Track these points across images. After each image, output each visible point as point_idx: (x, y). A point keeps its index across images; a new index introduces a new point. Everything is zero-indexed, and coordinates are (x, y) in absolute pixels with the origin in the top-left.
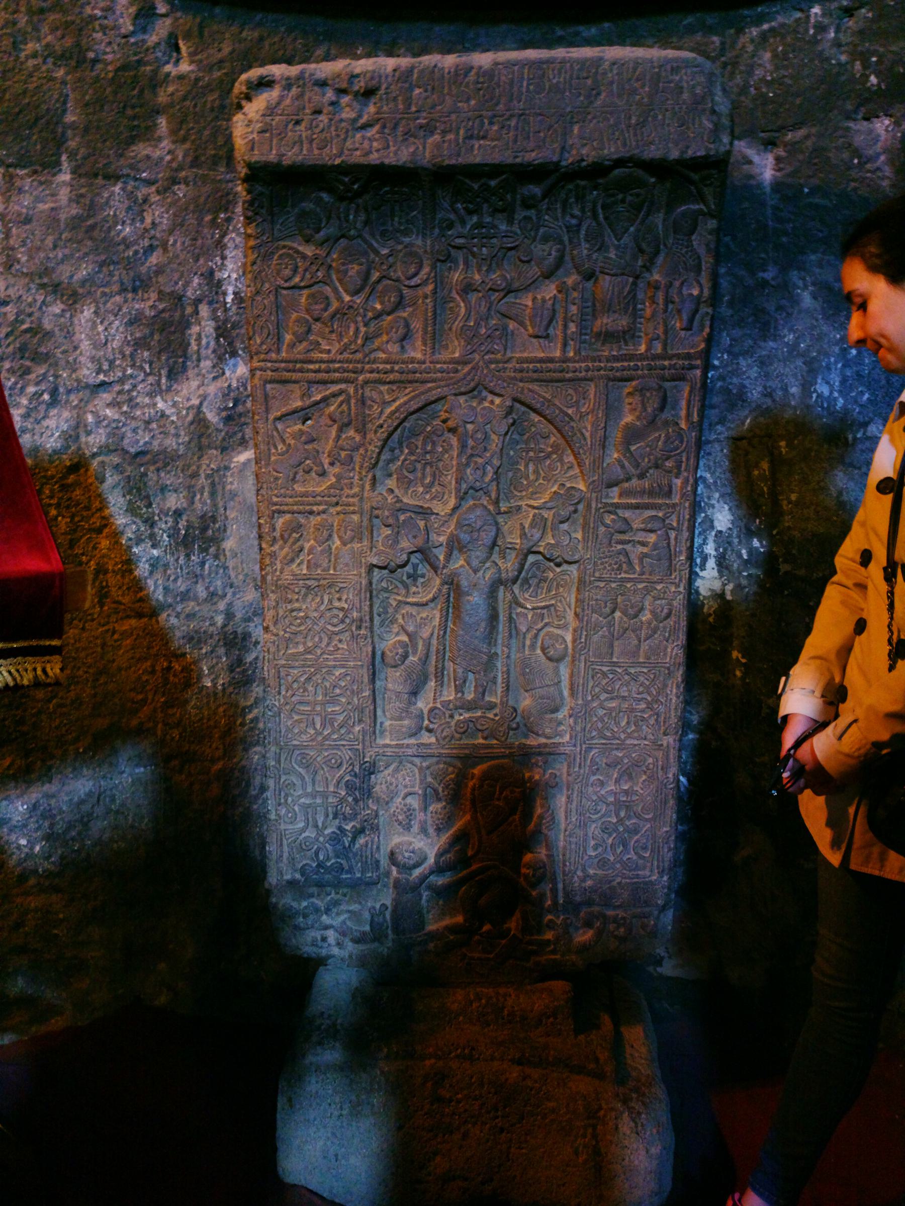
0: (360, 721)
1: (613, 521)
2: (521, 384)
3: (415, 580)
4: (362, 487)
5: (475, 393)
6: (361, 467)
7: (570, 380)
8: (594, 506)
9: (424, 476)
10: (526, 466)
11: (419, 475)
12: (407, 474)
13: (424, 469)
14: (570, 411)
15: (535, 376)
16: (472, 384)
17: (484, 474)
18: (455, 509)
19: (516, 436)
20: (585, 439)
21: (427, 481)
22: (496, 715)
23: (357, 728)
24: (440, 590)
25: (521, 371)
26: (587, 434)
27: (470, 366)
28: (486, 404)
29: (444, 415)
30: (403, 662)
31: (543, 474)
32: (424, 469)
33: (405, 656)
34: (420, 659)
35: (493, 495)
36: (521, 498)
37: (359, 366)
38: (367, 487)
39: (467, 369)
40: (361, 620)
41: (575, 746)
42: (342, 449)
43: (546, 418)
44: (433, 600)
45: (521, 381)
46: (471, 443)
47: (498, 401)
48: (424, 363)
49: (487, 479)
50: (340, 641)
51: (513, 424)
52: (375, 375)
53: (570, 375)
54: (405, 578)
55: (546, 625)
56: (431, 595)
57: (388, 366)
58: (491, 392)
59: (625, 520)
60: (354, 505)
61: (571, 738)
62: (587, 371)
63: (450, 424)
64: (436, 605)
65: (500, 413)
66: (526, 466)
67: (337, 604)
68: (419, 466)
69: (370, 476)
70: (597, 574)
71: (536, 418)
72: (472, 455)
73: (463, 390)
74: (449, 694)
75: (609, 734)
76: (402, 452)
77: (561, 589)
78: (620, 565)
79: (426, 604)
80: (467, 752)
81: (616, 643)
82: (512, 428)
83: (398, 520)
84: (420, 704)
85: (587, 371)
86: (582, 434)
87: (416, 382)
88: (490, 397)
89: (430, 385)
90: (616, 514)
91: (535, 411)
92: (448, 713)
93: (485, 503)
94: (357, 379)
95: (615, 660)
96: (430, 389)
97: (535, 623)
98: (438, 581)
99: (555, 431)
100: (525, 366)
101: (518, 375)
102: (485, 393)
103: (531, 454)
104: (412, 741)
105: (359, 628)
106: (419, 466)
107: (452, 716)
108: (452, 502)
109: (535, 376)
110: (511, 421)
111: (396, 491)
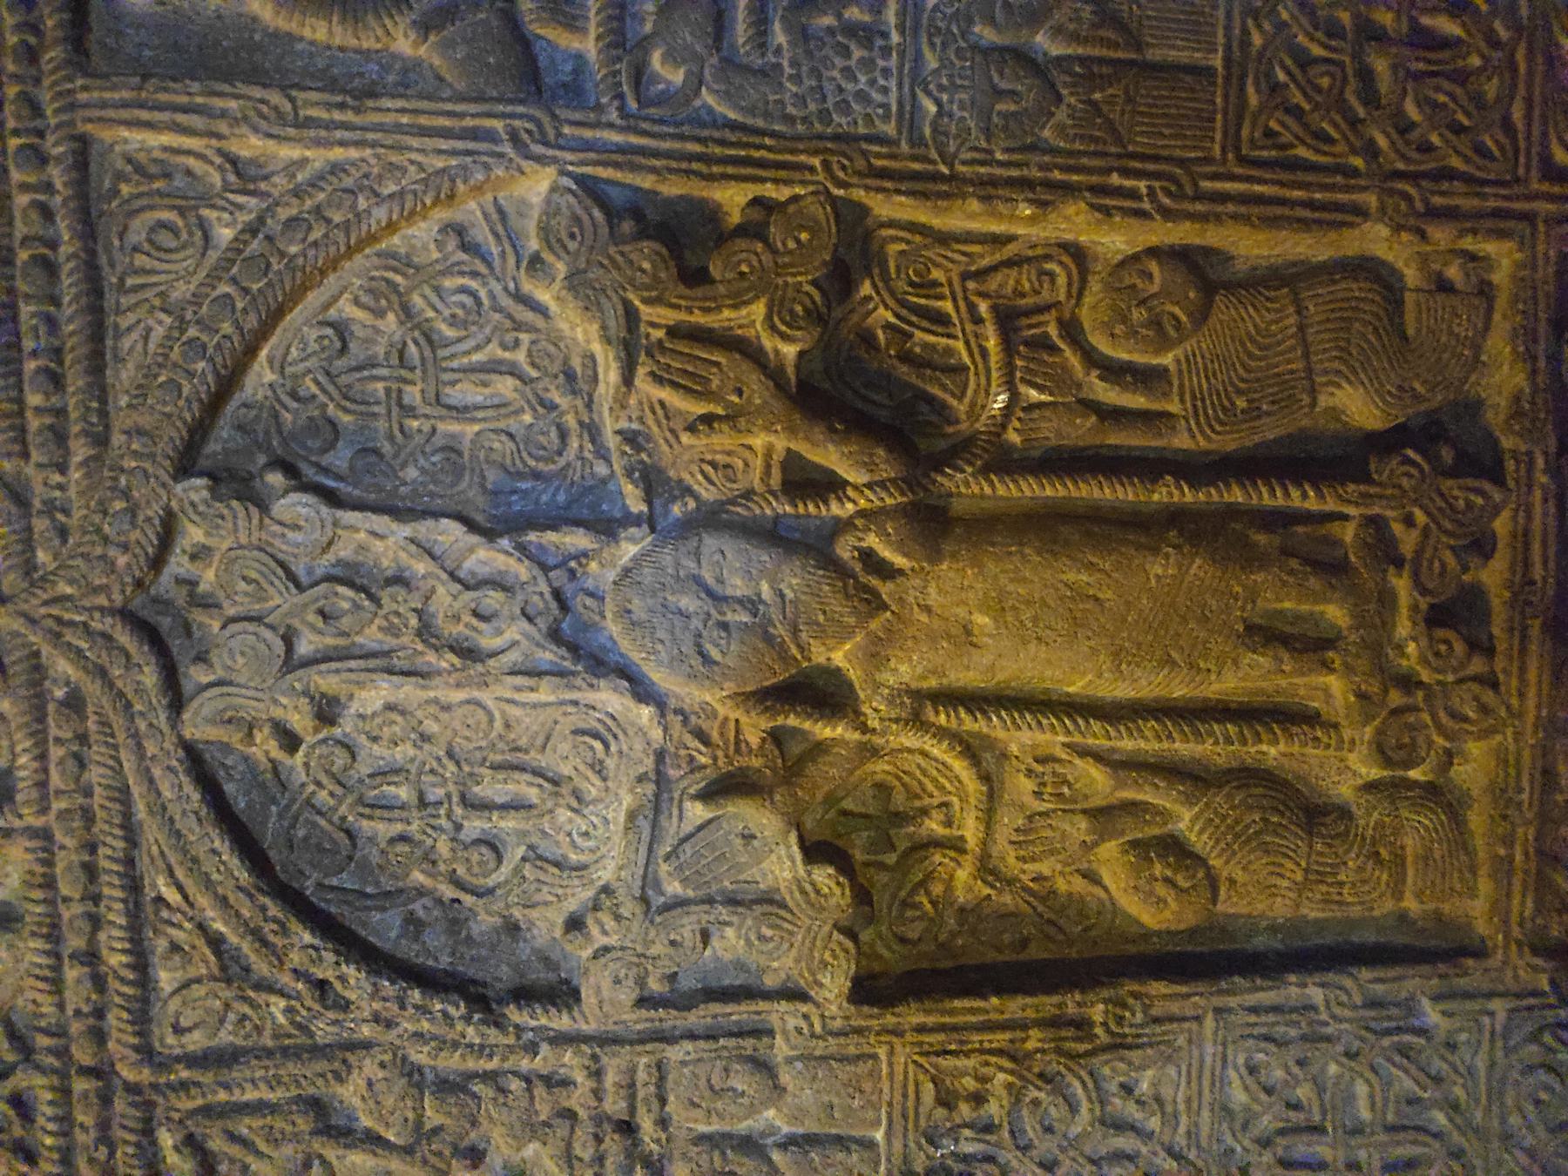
0: (1409, 1006)
1: (671, 57)
2: (117, 439)
3: (899, 818)
4: (562, 1040)
5: (165, 623)
6: (482, 1050)
7: (88, 230)
8: (616, 138)
9: (516, 806)
10: (462, 412)
11: (508, 824)
12: (505, 870)
13: (485, 807)
14: (225, 234)
15: (76, 380)
16: (124, 638)
17: (498, 583)
18: (642, 691)
19: (340, 459)
20: (336, 169)
21: (533, 794)
22: (1409, 521)
23: (1432, 1015)
24: (941, 733)
25: (59, 436)
26: (319, 158)
27: (46, 650)
28: (208, 578)
29: (265, 747)
30: (1200, 861)
31: (494, 350)
32: (485, 807)
33: (1174, 848)
34: (1189, 801)
35: (577, 540)
36: (592, 431)
37: (80, 1085)
38: (562, 1022)
39: (63, 667)
40: (1054, 1023)
41: (1529, 217)
42: (419, 1124)
43: (264, 332)
44: (970, 749)
45: (101, 440)
46: (372, 637)
47: (193, 534)
48: (45, 835)
49: (522, 571)
50: (1127, 1089)
51: (290, 470)
52: (116, 1019)
53: (64, 228)
54: (891, 859)
55: (1072, 330)
56: (959, 766)
57: (72, 973)
58: (157, 563)
60: (632, 1071)
61: (1502, 235)
62: (43, 160)
63: (299, 720)
64: (989, 743)
65: (239, 523)
66: (462, 412)
67: (993, 1109)
68: (475, 826)
69: (515, 1015)
70: (890, 129)
71: (261, 376)
72: (426, 631)
73: (150, 677)
74: (1331, 689)
75: (1491, 89)
76: (421, 892)
77: (936, 274)
78: (851, 30)
79: (986, 778)
80: (1535, 627)
81: (1154, 55)
82: (309, 472)
83: (680, 903)
84: (1345, 791)
85: (43, 160)
86: (314, 184)
87: (130, 862)
88: (178, 564)
89: (141, 811)
90: (645, 44)
91: (228, 383)
92: (1396, 698)
93: (611, 575)
94: (132, 1089)
95: (1217, 61)
96: (160, 809)
97: (1060, 380)
98: (910, 740)
99: (314, 299)
100: (34, 423)
101: (80, 451)
102: (165, 583)
103: (413, 394)
104: (1476, 820)
105: (1082, 1025)
106: (475, 826)
107: (1408, 683)
108: (610, 698)
109: (76, 380)
110: (276, 479)
111: (572, 905)
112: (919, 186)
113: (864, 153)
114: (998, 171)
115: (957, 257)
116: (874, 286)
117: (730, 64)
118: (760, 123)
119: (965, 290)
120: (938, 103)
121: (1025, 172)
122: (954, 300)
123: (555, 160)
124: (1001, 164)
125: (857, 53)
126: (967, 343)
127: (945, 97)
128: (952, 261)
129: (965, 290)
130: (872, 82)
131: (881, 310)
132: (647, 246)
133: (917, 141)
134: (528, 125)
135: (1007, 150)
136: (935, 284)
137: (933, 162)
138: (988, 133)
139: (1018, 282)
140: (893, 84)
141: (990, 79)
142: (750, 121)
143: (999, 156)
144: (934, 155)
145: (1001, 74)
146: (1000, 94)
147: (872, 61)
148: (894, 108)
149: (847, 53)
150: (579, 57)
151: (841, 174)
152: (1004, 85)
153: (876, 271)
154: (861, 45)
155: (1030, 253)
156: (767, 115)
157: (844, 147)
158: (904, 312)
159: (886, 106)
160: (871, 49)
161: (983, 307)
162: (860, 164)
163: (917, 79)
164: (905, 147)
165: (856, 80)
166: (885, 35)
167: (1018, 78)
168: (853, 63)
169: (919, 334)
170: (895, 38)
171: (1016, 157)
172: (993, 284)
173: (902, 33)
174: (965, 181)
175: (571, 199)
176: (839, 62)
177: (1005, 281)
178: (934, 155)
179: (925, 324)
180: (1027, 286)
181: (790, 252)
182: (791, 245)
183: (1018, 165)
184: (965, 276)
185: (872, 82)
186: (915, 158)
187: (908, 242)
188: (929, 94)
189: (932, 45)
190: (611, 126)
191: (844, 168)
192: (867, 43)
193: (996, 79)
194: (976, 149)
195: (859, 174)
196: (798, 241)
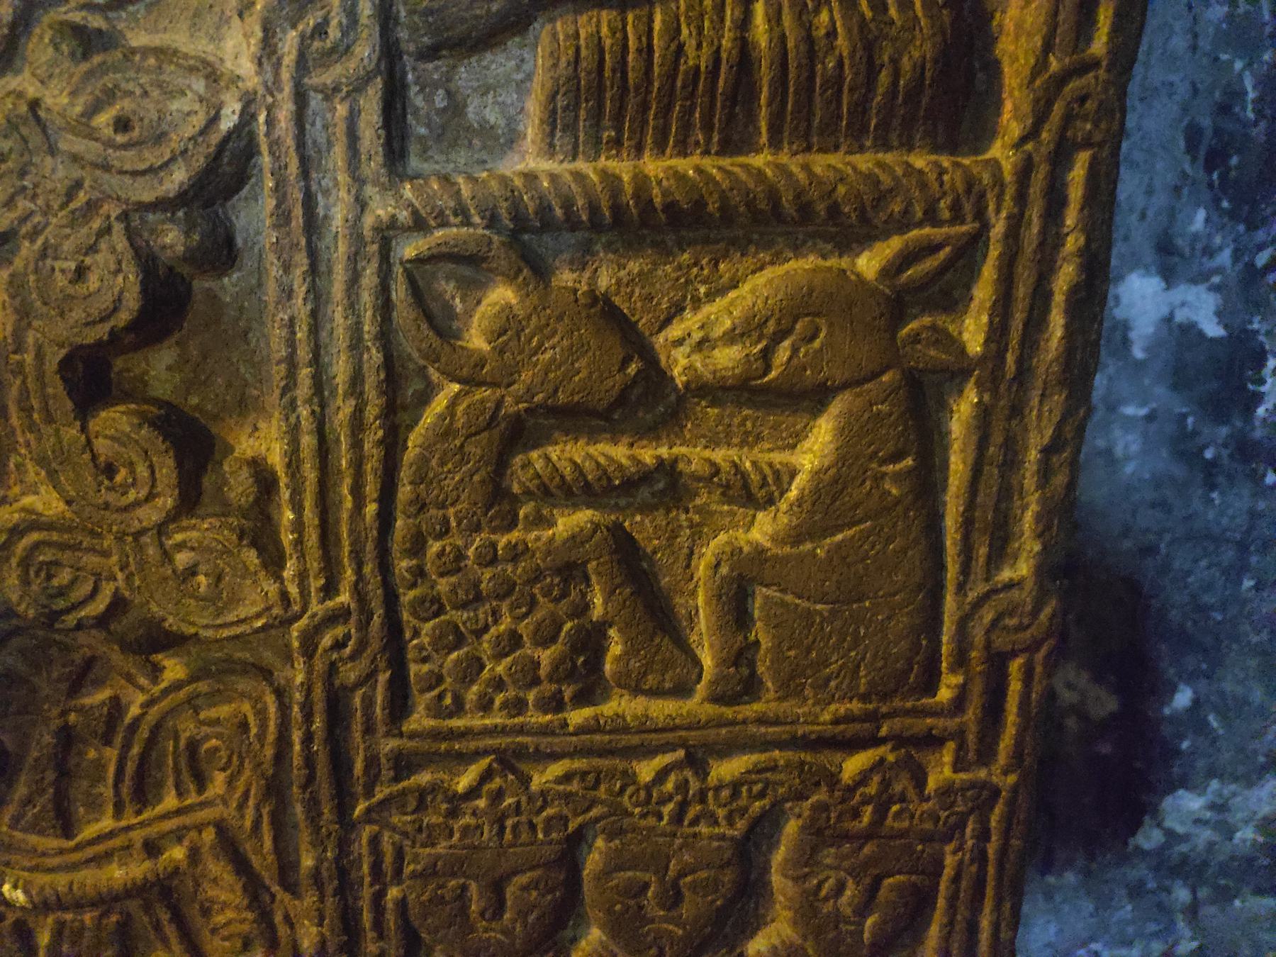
1: (507, 328)
8: (338, 213)
59: (606, 312)
70: (419, 720)
77: (218, 782)
78: (590, 642)
112: (322, 770)
113: (370, 676)
114: (367, 893)
115: (250, 813)
116: (177, 686)
117: (517, 434)
118: (405, 491)
119: (199, 828)
120: (473, 793)
121: (371, 935)
122: (179, 812)
123: (272, 88)
124: (379, 897)
125: (546, 656)
126: (111, 834)
127: (482, 803)
128: (241, 806)
129: (199, 828)
130: (499, 684)
131: (141, 698)
132: (129, 284)
133: (404, 765)
134: (334, 33)
135: (402, 904)
136: (201, 781)
137: (369, 793)
138: (428, 874)
139: (225, 906)
140: (496, 719)
141: (515, 873)
142: (405, 474)
143: (393, 893)
144: (381, 793)
145: (525, 888)
146: (497, 888)
147: (536, 681)
148: (457, 723)
149: (545, 640)
150: (512, 139)
151: (327, 641)
152: (510, 891)
153: (203, 686)
154: (556, 665)
155: (278, 918)
156: (420, 505)
157: (375, 645)
158: (144, 733)
159: (459, 708)
160: (551, 679)
161: (178, 853)
162: (350, 673)
163: (510, 761)
164: (389, 745)
165: (499, 656)
166: (584, 698)
167: (522, 914)
168: (528, 650)
169: (111, 754)
170: (577, 717)
171: (391, 919)
172: (217, 868)
173: (581, 730)
174: (343, 845)
175: (199, 121)
176: (524, 628)
177: (222, 888)
178: (381, 793)
179: (130, 767)
180: (220, 919)
181: (167, 556)
182: (182, 559)
183: (378, 924)
184: (221, 827)
185: (499, 684)
186: (372, 762)
187: (261, 736)
188: (486, 776)
189: (567, 778)
190: (361, 204)
191: (339, 645)
192: (563, 671)
193: (523, 879)
194: (399, 855)
195: (332, 668)
196: (192, 571)
